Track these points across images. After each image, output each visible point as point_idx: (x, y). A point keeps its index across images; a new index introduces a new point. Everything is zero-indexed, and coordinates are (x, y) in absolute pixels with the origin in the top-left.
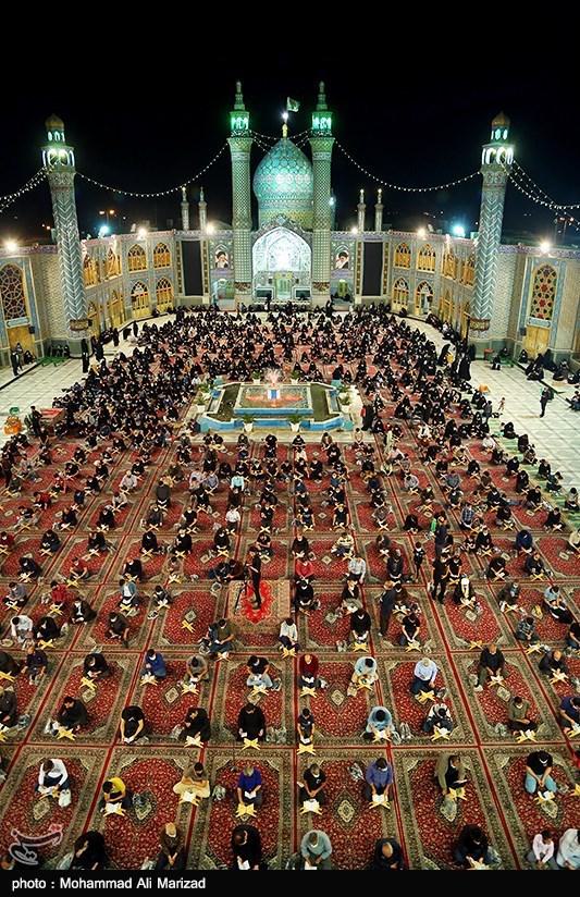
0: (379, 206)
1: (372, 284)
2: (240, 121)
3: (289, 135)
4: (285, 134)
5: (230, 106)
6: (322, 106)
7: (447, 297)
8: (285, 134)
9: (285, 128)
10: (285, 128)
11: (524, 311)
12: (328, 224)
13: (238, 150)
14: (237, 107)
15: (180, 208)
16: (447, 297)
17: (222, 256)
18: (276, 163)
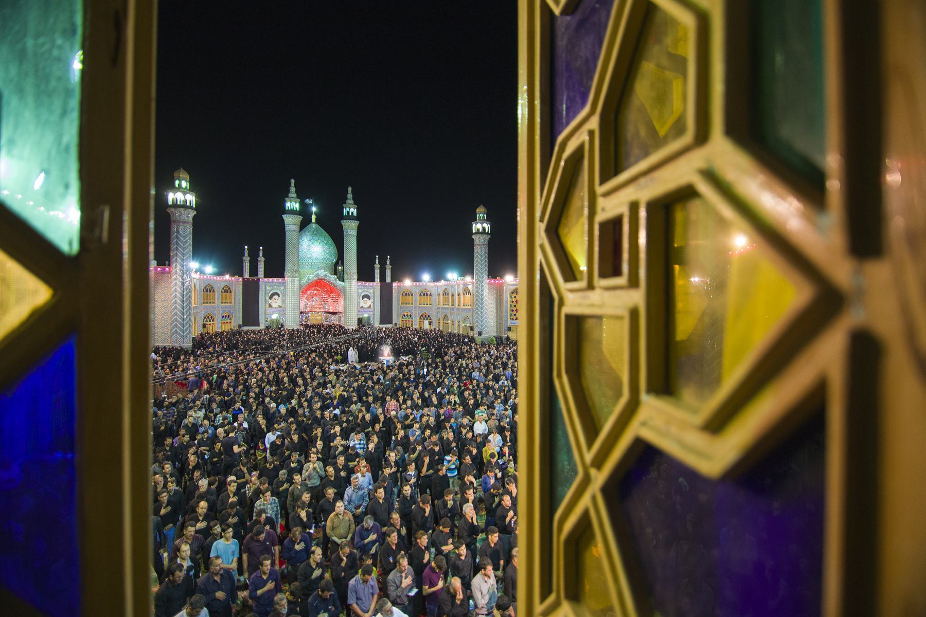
0: (388, 267)
1: (386, 316)
2: (293, 204)
3: (317, 221)
4: (314, 220)
5: (286, 194)
6: (352, 202)
7: (445, 317)
8: (314, 220)
9: (314, 217)
10: (314, 217)
11: (506, 316)
12: (356, 277)
13: (291, 222)
14: (290, 195)
15: (242, 262)
16: (445, 317)
17: (276, 297)
18: (309, 237)
